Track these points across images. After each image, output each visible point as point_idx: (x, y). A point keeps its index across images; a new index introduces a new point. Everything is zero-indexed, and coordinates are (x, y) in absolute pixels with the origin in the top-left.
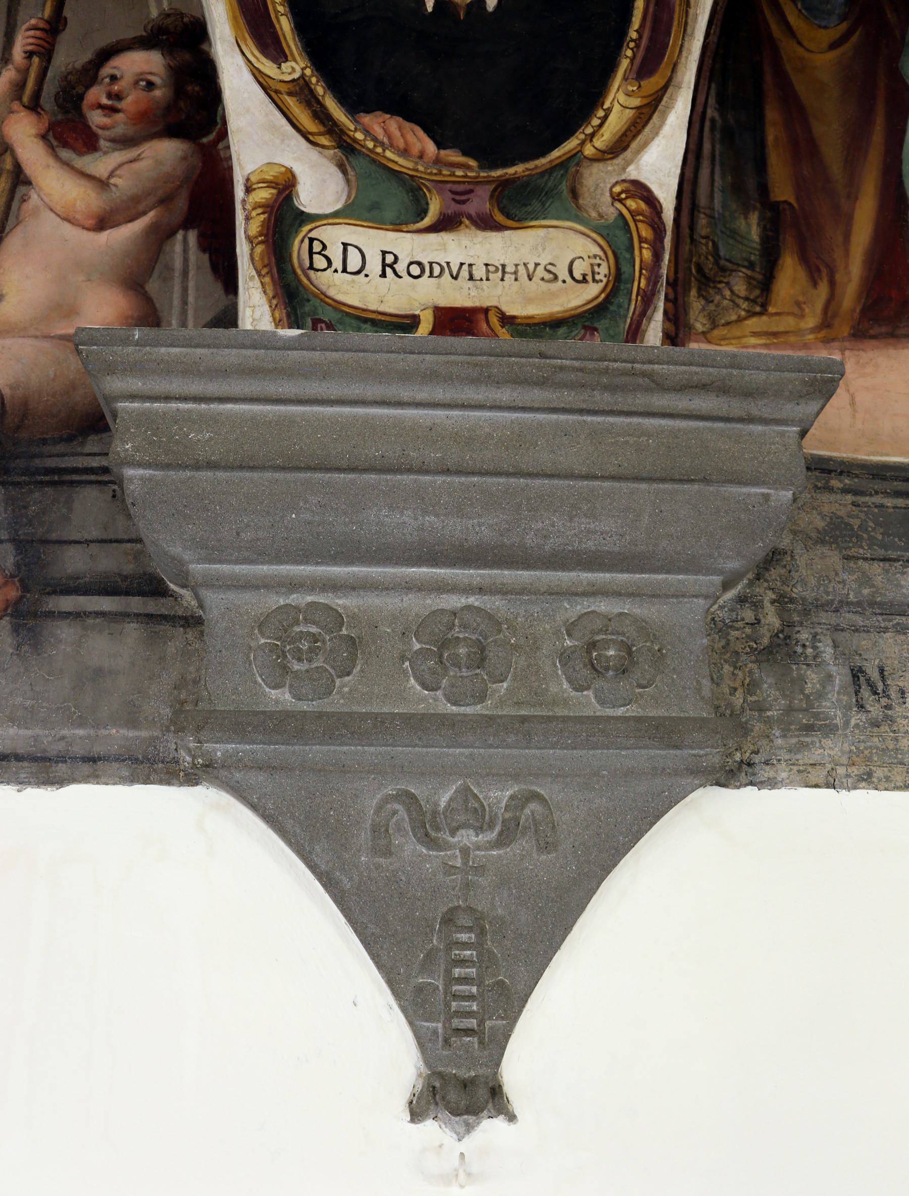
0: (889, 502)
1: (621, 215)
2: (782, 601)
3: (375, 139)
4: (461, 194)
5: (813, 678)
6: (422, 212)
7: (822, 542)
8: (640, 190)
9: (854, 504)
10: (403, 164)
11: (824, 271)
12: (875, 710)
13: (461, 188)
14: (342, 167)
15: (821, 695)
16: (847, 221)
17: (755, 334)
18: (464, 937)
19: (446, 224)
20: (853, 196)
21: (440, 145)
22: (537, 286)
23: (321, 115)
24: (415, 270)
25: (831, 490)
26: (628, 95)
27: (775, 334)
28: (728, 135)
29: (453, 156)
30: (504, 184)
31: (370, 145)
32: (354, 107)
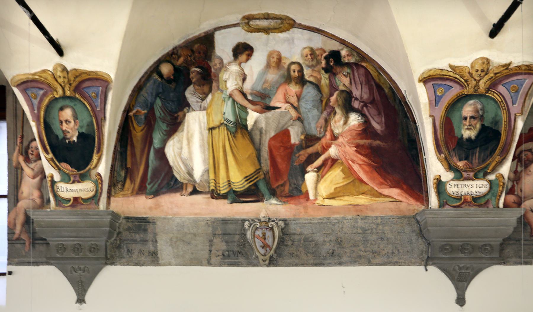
0: (137, 223)
1: (97, 179)
2: (120, 240)
3: (63, 168)
4: (75, 177)
5: (122, 250)
6: (70, 180)
7: (126, 230)
8: (99, 174)
9: (132, 224)
10: (67, 171)
11: (133, 181)
12: (130, 255)
13: (74, 175)
14: (59, 173)
15: (123, 253)
16: (138, 170)
17: (121, 195)
18: (80, 283)
19: (73, 182)
20: (140, 165)
21: (72, 167)
22: (86, 193)
23: (55, 164)
24: (70, 191)
25: (129, 222)
26: (96, 157)
27: (124, 195)
28: (121, 154)
29: (74, 170)
30: (81, 174)
31: (62, 168)
32: (60, 162)
